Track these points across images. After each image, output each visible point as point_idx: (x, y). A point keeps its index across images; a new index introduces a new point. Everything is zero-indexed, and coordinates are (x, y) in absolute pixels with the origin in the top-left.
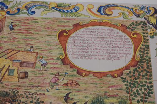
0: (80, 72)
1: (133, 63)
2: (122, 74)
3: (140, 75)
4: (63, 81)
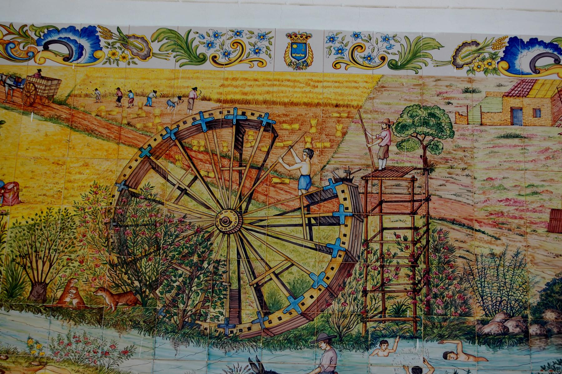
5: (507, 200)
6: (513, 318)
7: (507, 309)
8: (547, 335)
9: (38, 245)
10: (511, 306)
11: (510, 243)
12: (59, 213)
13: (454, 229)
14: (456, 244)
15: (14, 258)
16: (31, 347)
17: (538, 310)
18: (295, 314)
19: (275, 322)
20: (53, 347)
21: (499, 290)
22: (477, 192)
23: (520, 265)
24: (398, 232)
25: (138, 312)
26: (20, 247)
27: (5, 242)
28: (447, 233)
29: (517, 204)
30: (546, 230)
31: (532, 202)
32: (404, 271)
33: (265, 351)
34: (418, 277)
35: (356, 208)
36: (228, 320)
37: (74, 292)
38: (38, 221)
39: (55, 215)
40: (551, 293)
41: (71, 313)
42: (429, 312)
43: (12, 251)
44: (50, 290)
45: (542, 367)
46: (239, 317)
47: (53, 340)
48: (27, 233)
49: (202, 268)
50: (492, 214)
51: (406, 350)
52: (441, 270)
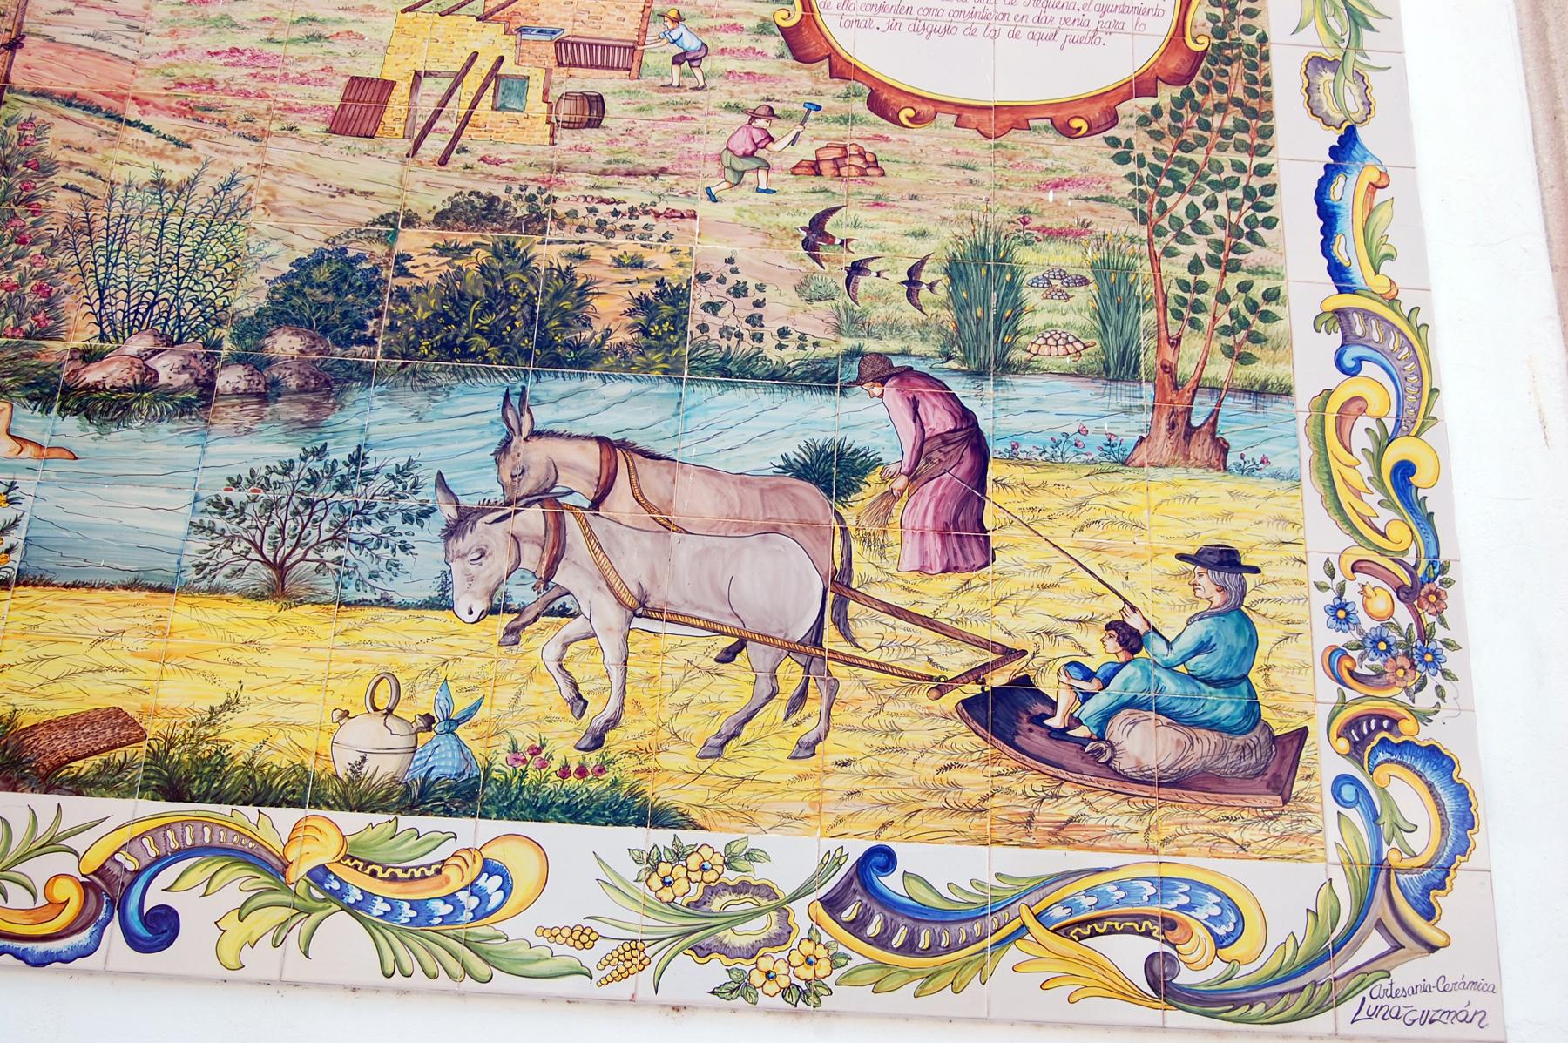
0: (882, 102)
1: (1174, 63)
2: (1113, 121)
3: (1206, 126)
4: (790, 148)
5: (234, 51)
6: (177, 348)
7: (166, 323)
8: (265, 394)
10: (179, 315)
11: (216, 156)
13: (67, 118)
14: (63, 156)
17: (255, 329)
21: (155, 274)
22: (155, 31)
23: (232, 211)
28: (47, 126)
29: (261, 62)
30: (325, 126)
31: (304, 59)
40: (303, 285)
45: (230, 479)
50: (182, 85)
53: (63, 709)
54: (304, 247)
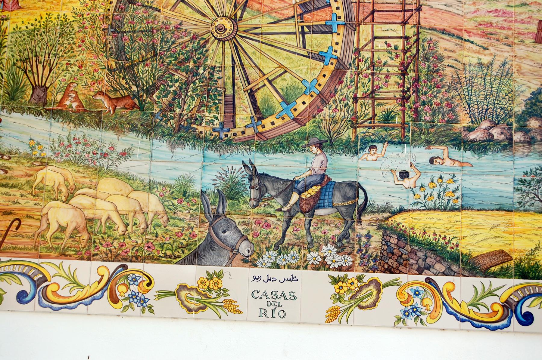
5: (496, 10)
6: (498, 126)
7: (493, 117)
8: (530, 142)
9: (38, 49)
10: (496, 114)
11: (498, 53)
12: (58, 18)
13: (443, 39)
14: (445, 54)
15: (15, 62)
16: (33, 148)
17: (523, 118)
18: (287, 119)
19: (268, 127)
20: (53, 148)
21: (485, 98)
22: (467, 3)
23: (507, 74)
24: (389, 41)
25: (136, 116)
26: (20, 51)
27: (6, 46)
28: (437, 42)
29: (506, 15)
30: (533, 40)
31: (521, 13)
32: (393, 79)
33: (258, 154)
34: (407, 85)
35: (348, 17)
36: (222, 124)
37: (74, 95)
38: (38, 27)
39: (54, 21)
40: (536, 102)
41: (71, 116)
42: (417, 117)
43: (13, 56)
44: (50, 93)
45: (524, 172)
46: (234, 121)
47: (53, 141)
48: (27, 38)
49: (197, 74)
50: (481, 25)
51: (394, 154)
52: (430, 78)
53: (485, 251)
54: (534, 88)
